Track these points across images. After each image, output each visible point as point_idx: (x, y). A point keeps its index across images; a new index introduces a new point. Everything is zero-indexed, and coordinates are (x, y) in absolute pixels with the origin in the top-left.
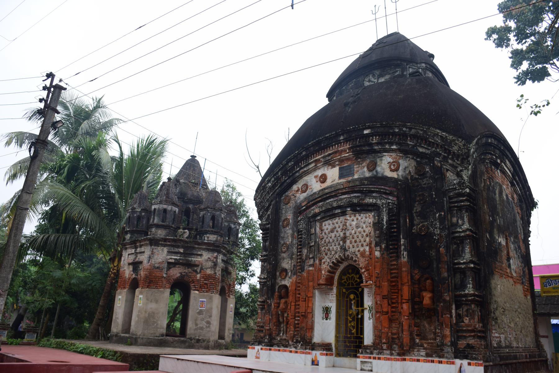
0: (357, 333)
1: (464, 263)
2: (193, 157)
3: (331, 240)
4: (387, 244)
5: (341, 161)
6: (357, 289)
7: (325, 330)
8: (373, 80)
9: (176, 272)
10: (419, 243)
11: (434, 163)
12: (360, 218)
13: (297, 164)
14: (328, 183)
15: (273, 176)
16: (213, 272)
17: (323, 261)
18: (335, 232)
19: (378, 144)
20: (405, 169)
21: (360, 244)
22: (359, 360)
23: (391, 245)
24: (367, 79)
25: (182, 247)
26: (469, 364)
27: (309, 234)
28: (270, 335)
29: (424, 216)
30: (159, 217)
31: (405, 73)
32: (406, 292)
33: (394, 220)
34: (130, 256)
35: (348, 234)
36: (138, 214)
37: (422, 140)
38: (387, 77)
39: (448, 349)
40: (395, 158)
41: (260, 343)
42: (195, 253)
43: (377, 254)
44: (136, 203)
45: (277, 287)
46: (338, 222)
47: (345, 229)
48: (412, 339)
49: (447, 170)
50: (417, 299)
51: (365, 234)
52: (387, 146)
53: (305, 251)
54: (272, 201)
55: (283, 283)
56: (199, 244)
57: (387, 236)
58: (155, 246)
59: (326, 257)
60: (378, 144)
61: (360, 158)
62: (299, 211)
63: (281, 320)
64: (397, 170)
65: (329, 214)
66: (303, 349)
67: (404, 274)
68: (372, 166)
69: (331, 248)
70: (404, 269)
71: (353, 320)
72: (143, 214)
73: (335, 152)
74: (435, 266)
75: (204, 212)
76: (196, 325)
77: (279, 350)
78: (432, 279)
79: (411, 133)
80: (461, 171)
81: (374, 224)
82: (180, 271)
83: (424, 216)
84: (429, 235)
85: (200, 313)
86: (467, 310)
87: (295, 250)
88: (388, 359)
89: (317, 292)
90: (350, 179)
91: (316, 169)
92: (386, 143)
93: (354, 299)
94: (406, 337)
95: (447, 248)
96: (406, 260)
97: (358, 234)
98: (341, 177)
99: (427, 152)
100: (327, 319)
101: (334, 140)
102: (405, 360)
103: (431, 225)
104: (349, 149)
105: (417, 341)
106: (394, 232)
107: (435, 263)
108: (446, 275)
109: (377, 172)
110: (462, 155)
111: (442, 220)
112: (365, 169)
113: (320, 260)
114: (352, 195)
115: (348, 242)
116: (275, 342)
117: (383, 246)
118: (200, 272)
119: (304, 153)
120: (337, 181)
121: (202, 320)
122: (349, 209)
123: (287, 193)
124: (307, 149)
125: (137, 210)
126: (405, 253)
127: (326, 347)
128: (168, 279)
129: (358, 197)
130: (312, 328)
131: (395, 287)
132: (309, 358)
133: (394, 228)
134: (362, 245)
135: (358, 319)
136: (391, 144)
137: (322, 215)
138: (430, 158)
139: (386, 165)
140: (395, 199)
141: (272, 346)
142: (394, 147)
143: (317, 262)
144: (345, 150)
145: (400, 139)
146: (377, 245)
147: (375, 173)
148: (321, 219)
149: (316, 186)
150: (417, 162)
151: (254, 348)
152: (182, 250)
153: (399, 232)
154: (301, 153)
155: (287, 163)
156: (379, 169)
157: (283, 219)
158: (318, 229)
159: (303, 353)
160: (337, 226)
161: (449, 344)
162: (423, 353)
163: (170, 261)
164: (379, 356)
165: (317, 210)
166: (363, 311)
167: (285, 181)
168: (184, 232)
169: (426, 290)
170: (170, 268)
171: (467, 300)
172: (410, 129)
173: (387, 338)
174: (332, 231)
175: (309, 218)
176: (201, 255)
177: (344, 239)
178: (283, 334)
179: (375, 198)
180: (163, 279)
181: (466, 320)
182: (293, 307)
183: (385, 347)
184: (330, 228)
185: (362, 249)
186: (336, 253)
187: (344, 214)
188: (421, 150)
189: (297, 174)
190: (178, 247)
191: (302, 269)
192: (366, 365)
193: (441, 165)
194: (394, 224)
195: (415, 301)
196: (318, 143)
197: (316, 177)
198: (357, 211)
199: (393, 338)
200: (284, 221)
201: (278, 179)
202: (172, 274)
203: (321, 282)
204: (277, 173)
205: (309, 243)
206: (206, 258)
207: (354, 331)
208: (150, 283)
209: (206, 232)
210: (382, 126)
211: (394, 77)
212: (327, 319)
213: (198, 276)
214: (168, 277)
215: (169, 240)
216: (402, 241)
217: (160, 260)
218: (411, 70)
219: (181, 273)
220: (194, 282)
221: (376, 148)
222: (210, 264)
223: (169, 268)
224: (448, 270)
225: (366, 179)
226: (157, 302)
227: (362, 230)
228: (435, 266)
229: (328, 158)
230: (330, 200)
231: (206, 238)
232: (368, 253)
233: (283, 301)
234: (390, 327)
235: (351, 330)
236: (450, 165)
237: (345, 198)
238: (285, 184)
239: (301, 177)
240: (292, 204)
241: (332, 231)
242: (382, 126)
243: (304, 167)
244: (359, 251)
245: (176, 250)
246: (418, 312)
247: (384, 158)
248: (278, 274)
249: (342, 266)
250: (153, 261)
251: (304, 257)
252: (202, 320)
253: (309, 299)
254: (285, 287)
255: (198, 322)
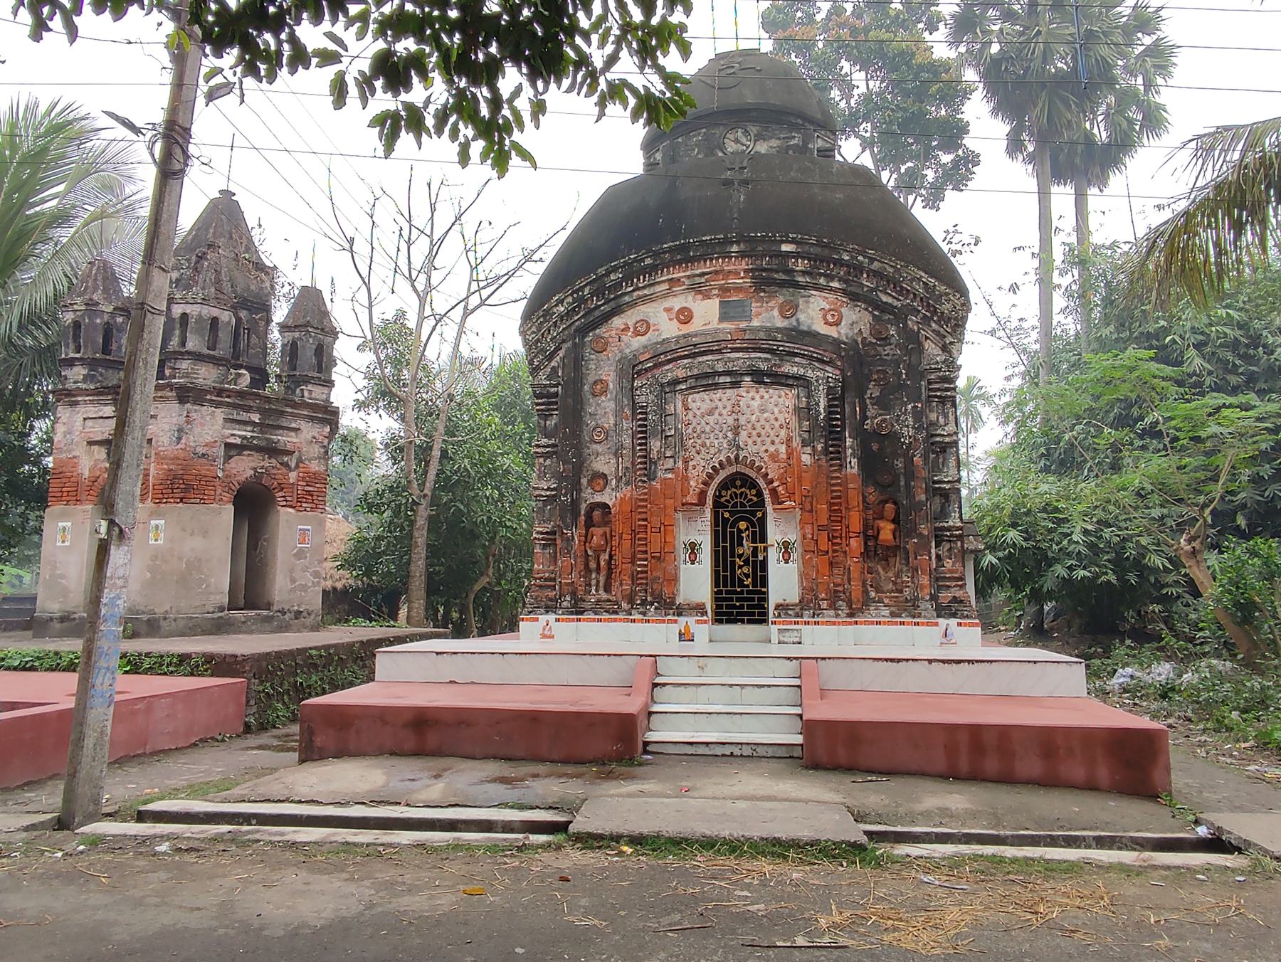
0: (755, 585)
1: (949, 482)
2: (227, 194)
3: (708, 429)
4: (826, 443)
5: (725, 290)
6: (753, 513)
7: (696, 581)
8: (744, 140)
9: (244, 467)
10: (875, 447)
11: (906, 325)
12: (766, 396)
13: (628, 278)
14: (696, 325)
15: (571, 295)
16: (323, 468)
17: (691, 463)
18: (716, 415)
19: (804, 273)
20: (852, 324)
21: (769, 440)
22: (774, 628)
23: (832, 446)
24: (732, 137)
25: (258, 410)
26: (960, 624)
27: (663, 414)
28: (573, 594)
29: (883, 404)
30: (203, 337)
31: (810, 146)
32: (855, 520)
33: (836, 406)
34: (89, 423)
35: (742, 421)
36: (106, 317)
37: (888, 282)
38: (774, 143)
39: (926, 605)
40: (832, 303)
41: (548, 610)
42: (285, 424)
43: (806, 459)
44: (95, 289)
45: (583, 506)
46: (723, 398)
47: (736, 410)
48: (866, 592)
49: (927, 338)
50: (870, 532)
51: (777, 425)
52: (822, 281)
53: (655, 445)
54: (564, 341)
55: (598, 498)
56: (295, 405)
57: (828, 432)
58: (194, 404)
59: (698, 457)
60: (804, 273)
61: (764, 291)
62: (633, 369)
63: (593, 565)
64: (837, 324)
65: (706, 381)
66: (660, 615)
67: (852, 494)
68: (789, 310)
69: (708, 442)
70: (851, 486)
71: (746, 562)
72: (120, 320)
73: (716, 272)
74: (902, 483)
75: (297, 335)
76: (293, 581)
77: (600, 620)
78: (895, 503)
79: (872, 267)
80: (951, 343)
81: (798, 410)
82: (253, 465)
83: (883, 404)
84: (894, 437)
85: (300, 554)
86: (950, 549)
87: (627, 441)
88: (834, 623)
89: (680, 515)
90: (743, 325)
91: (669, 294)
92: (821, 275)
93: (747, 529)
94: (856, 588)
95: (925, 457)
96: (855, 471)
97: (762, 422)
98: (723, 317)
99: (896, 303)
100: (693, 563)
101: (718, 250)
102: (856, 623)
103: (897, 421)
104: (746, 271)
105: (873, 594)
106: (837, 426)
107: (902, 478)
108: (923, 497)
109: (797, 320)
110: (956, 319)
111: (918, 415)
112: (776, 313)
113: (686, 462)
114: (753, 355)
115: (744, 434)
116: (586, 605)
117: (819, 447)
118: (297, 467)
119: (648, 261)
120: (715, 324)
121: (305, 569)
122: (748, 379)
123: (597, 331)
124: (656, 255)
125: (104, 308)
126: (854, 461)
127: (700, 609)
128: (227, 482)
129: (766, 359)
130: (674, 580)
131: (837, 509)
132: (675, 629)
133: (837, 419)
134: (773, 442)
135: (755, 563)
136: (830, 278)
137: (691, 382)
138: (899, 316)
139: (816, 311)
140: (838, 372)
141: (582, 613)
142: (835, 284)
143: (680, 464)
144: (738, 270)
145: (849, 273)
146: (805, 443)
147: (795, 323)
148: (686, 389)
149: (669, 329)
150: (874, 316)
151: (537, 620)
152: (256, 418)
153: (843, 427)
154: (643, 260)
155: (608, 274)
156: (802, 317)
157: (591, 379)
158: (679, 405)
159: (663, 621)
160: (720, 404)
161: (928, 597)
162: (886, 612)
163: (231, 440)
164: (816, 619)
165: (681, 373)
166: (765, 549)
167: (598, 307)
168: (239, 375)
169: (882, 518)
170: (231, 457)
171: (952, 536)
172: (872, 260)
173: (828, 591)
174: (710, 413)
175: (662, 385)
176: (296, 430)
177: (736, 429)
178: (597, 590)
179: (799, 365)
180: (217, 482)
181: (948, 564)
182: (627, 544)
183: (824, 604)
184: (705, 406)
185: (772, 449)
186: (720, 451)
187: (735, 385)
188: (884, 298)
189: (627, 299)
190: (248, 409)
191: (651, 476)
192: (787, 634)
193: (919, 329)
194: (837, 413)
195: (870, 535)
196: (684, 248)
197: (668, 310)
198: (764, 383)
199: (836, 591)
200: (595, 383)
201: (582, 301)
202: (234, 471)
203: (689, 499)
204: (582, 289)
205: (663, 431)
206: (309, 437)
207: (748, 582)
208: (185, 491)
209: (306, 380)
210: (820, 244)
211: (788, 147)
212: (693, 563)
213: (293, 476)
214: (227, 476)
215: (229, 393)
216: (849, 442)
217: (209, 439)
218: (820, 143)
219: (255, 469)
220: (282, 489)
221: (800, 279)
222: (316, 450)
223: (228, 458)
224: (927, 491)
225: (778, 330)
226: (205, 534)
227: (772, 417)
228: (902, 483)
229: (698, 280)
230: (705, 358)
231: (306, 394)
232: (783, 456)
233: (597, 532)
234: (831, 575)
235: (741, 581)
236: (933, 331)
237: (739, 359)
238: (597, 313)
239: (632, 305)
240: (613, 353)
241: (710, 413)
242: (820, 244)
243: (644, 288)
244: (766, 451)
245: (244, 416)
246: (874, 551)
247: (812, 300)
248: (584, 481)
249: (723, 475)
250: (190, 440)
251: (654, 455)
252: (305, 569)
253: (666, 529)
254: (605, 506)
255: (297, 575)
